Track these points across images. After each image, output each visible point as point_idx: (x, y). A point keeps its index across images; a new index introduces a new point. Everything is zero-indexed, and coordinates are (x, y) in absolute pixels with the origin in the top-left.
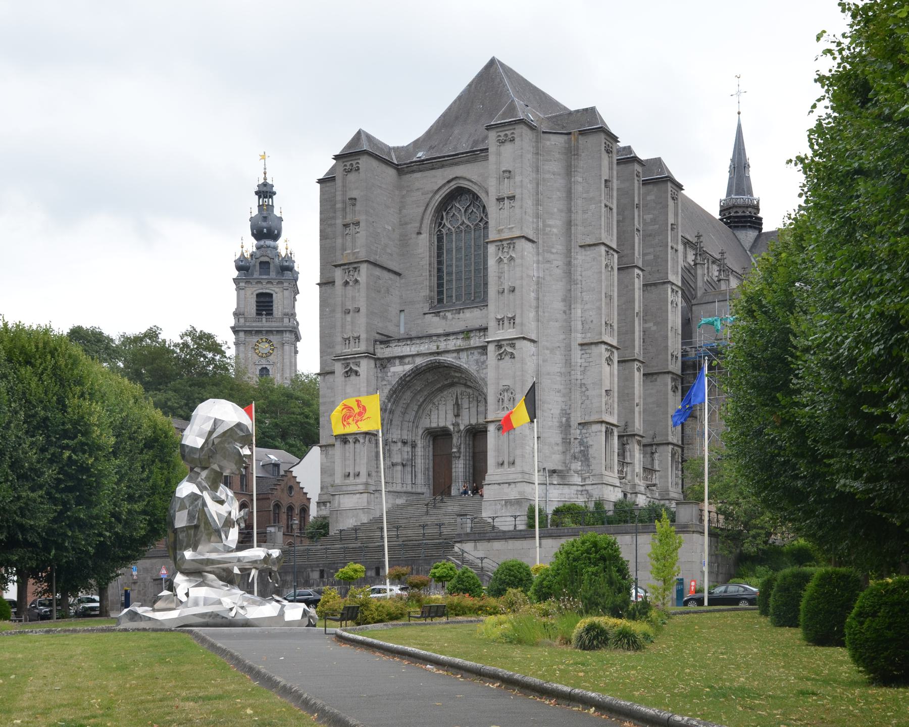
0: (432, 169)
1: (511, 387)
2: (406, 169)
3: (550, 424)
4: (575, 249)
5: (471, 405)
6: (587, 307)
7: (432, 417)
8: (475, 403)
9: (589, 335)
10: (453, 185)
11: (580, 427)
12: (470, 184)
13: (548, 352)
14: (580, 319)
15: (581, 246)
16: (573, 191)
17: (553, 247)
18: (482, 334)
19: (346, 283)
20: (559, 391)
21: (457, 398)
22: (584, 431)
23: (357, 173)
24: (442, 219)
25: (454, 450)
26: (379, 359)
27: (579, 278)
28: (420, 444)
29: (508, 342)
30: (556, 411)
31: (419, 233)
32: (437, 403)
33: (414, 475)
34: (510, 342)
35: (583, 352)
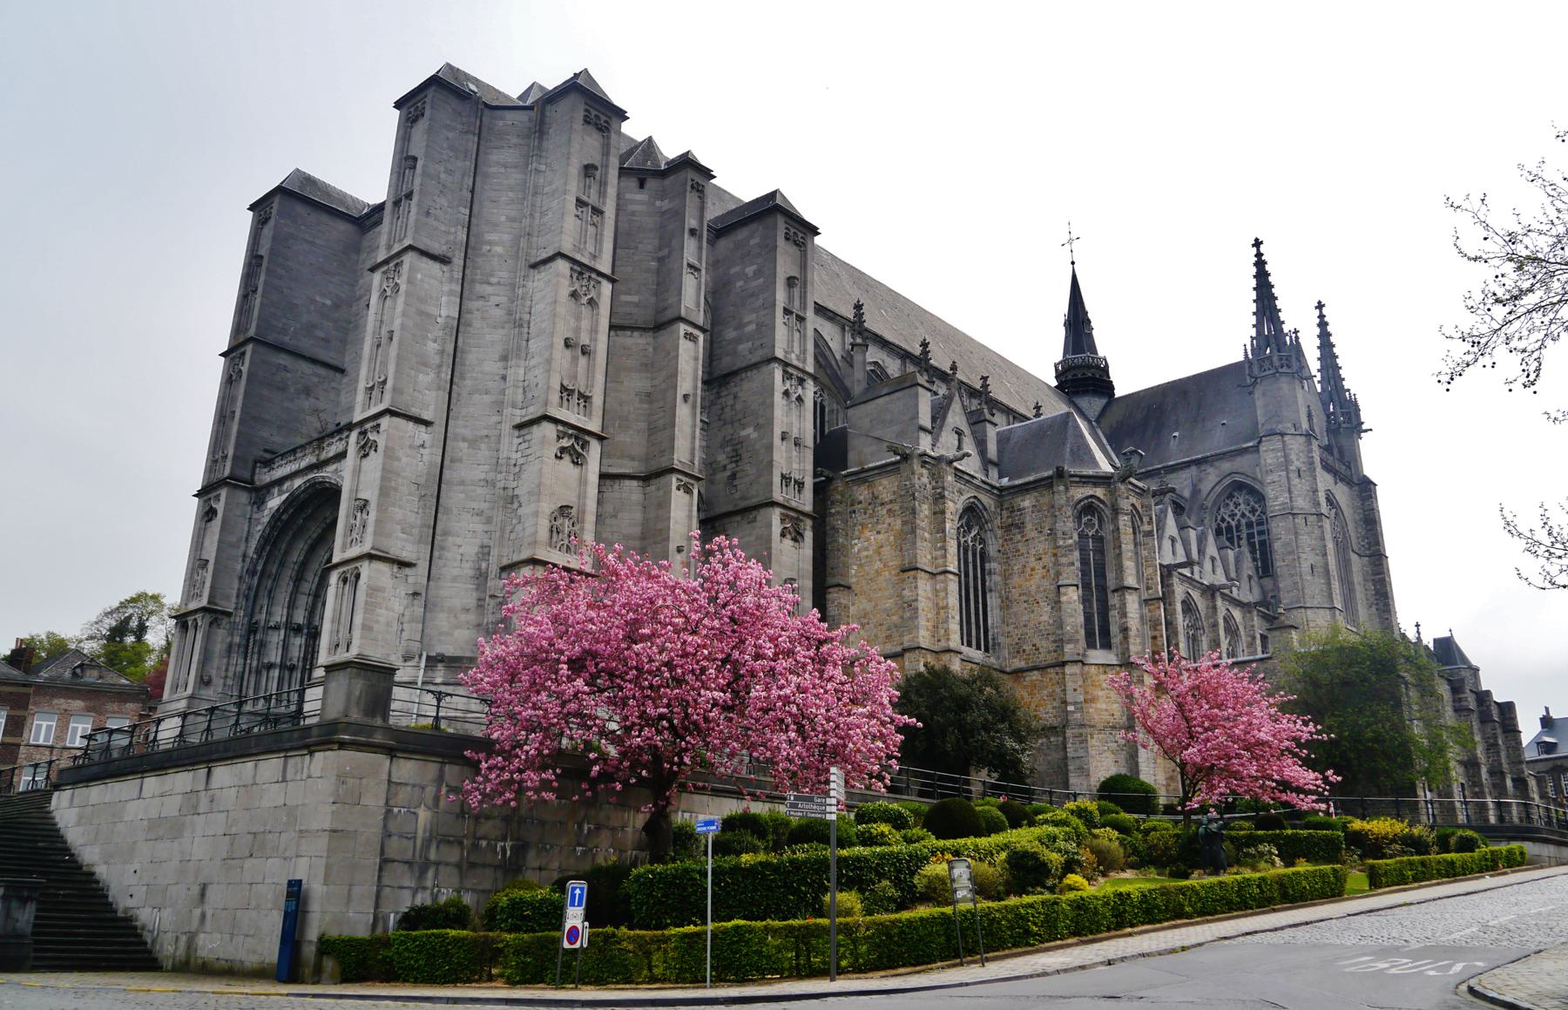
3: (456, 572)
9: (531, 409)
13: (466, 445)
14: (521, 384)
17: (492, 275)
20: (480, 514)
27: (526, 317)
30: (471, 549)
35: (520, 440)
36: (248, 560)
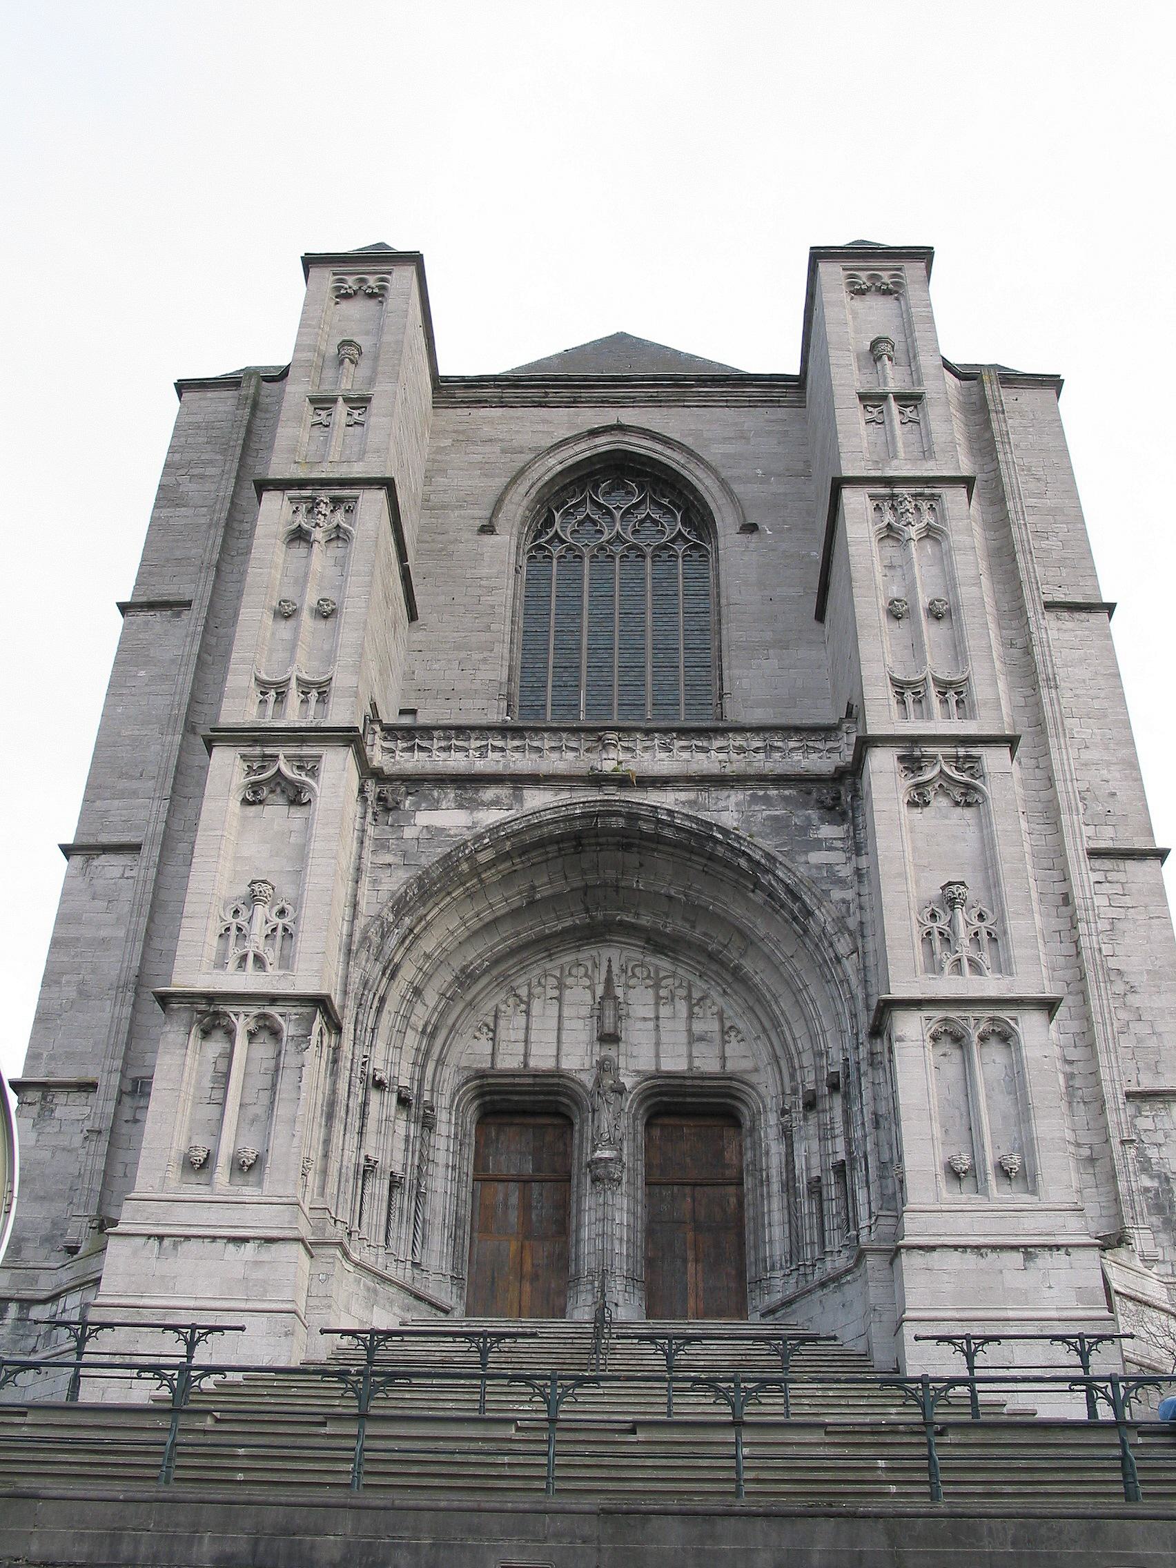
0: (541, 405)
1: (970, 895)
2: (460, 393)
4: (1033, 610)
5: (665, 1011)
6: (1086, 755)
7: (502, 1034)
8: (682, 1007)
10: (603, 444)
11: (1131, 1109)
12: (659, 447)
15: (1049, 606)
16: (1005, 480)
18: (792, 744)
19: (299, 536)
21: (609, 982)
22: (1144, 1123)
23: (372, 303)
24: (549, 522)
25: (607, 1154)
26: (378, 775)
28: (445, 1123)
29: (951, 751)
31: (487, 529)
32: (523, 992)
33: (419, 1224)
34: (962, 751)
35: (1099, 876)
36: (361, 922)
